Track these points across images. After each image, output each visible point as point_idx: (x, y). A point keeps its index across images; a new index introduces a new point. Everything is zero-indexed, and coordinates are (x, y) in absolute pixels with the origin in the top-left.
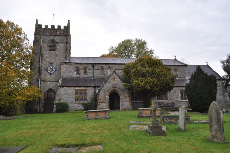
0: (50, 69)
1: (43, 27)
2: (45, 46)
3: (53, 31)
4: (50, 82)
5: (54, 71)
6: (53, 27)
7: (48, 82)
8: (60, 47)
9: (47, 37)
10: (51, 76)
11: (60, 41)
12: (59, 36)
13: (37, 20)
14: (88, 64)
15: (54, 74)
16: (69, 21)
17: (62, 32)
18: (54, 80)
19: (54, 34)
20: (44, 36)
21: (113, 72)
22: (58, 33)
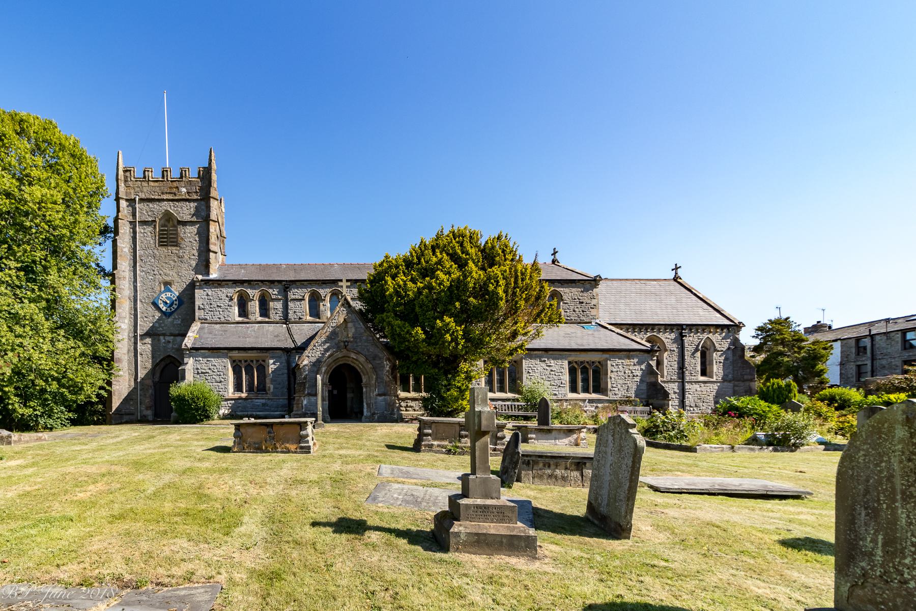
4: (167, 338)
7: (162, 338)
9: (151, 205)
10: (170, 320)
11: (187, 218)
14: (272, 282)
15: (176, 315)
18: (177, 332)
19: (171, 197)
22: (184, 190)
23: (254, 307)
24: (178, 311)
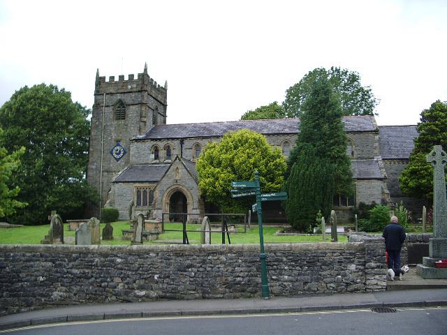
0: (120, 151)
1: (107, 80)
2: (108, 112)
3: (121, 85)
6: (121, 77)
12: (130, 92)
14: (173, 139)
16: (146, 66)
17: (135, 86)
19: (122, 91)
20: (108, 96)
21: (176, 159)
22: (130, 87)
23: (162, 153)
24: (124, 157)
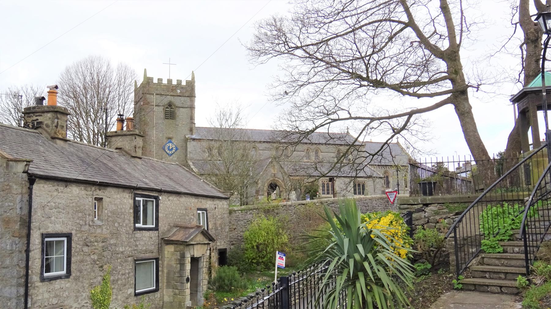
1: (155, 81)
5: (174, 151)
6: (170, 81)
8: (181, 113)
10: (171, 157)
12: (180, 96)
13: (145, 70)
15: (174, 155)
20: (157, 96)
22: (179, 91)
24: (176, 153)
